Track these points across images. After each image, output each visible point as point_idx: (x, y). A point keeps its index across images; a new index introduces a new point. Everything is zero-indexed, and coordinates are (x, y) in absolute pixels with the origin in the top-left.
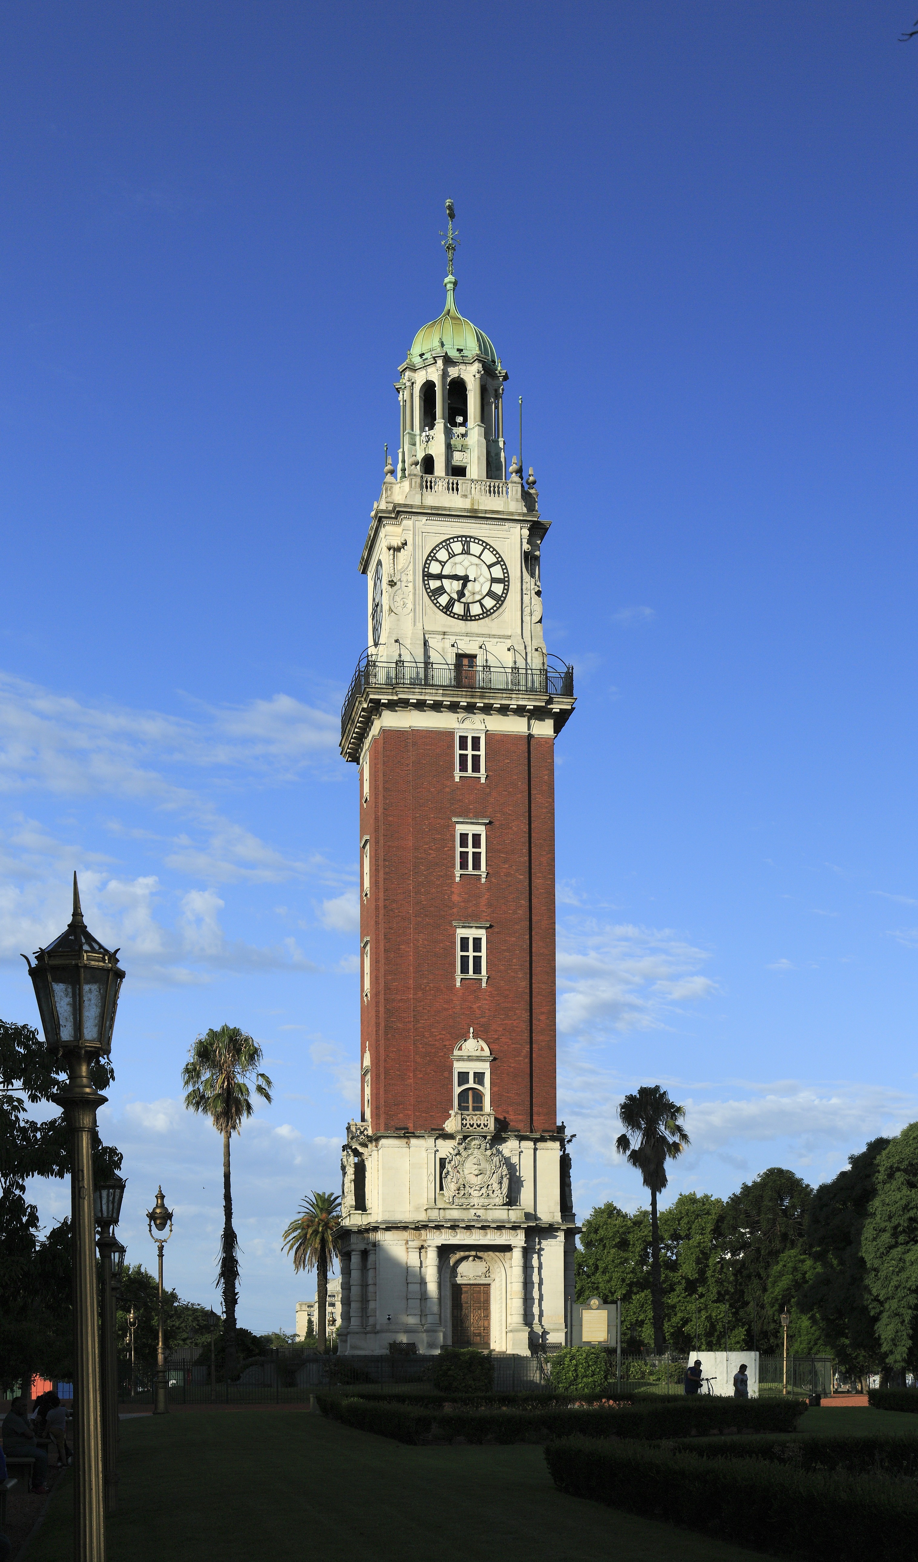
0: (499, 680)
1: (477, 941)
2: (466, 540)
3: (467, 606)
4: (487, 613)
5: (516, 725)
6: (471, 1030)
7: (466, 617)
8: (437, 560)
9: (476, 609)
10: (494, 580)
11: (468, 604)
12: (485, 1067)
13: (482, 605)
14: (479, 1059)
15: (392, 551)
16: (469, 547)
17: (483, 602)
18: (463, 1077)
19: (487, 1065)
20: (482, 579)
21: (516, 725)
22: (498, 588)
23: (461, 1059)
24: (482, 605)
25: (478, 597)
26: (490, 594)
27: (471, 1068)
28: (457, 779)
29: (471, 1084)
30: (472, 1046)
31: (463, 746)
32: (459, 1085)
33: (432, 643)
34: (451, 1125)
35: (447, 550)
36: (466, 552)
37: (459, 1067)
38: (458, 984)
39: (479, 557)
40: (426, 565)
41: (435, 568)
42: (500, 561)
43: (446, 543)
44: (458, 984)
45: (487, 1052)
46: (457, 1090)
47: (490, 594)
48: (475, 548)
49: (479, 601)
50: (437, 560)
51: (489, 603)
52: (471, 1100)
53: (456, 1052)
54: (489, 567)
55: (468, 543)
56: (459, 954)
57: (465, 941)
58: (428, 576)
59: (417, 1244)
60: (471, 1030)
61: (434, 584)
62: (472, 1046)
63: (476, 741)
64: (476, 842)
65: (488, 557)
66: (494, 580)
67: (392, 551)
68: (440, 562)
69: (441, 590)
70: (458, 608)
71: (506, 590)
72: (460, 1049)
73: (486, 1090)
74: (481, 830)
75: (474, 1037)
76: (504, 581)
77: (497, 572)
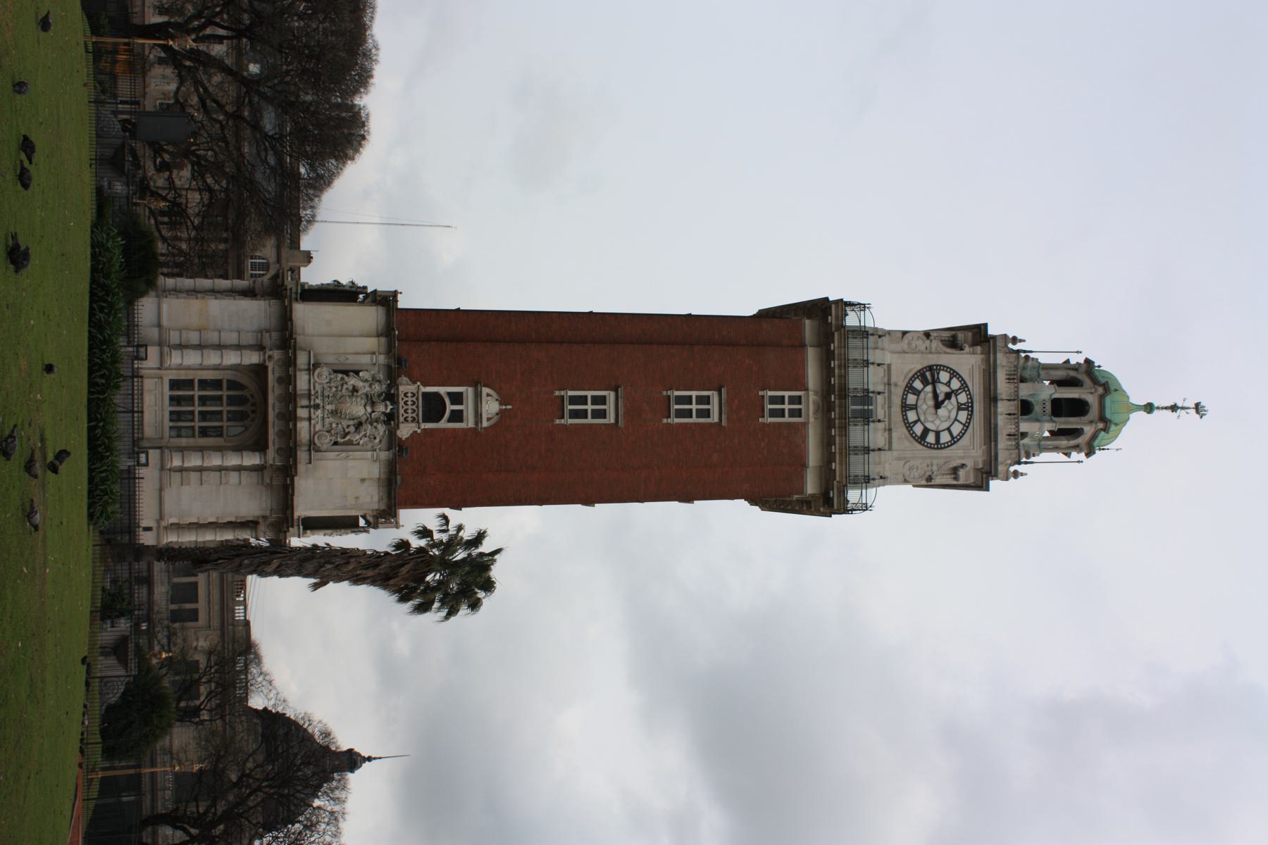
0: (856, 435)
1: (602, 414)
2: (969, 407)
3: (914, 407)
4: (909, 426)
5: (813, 457)
7: (905, 407)
9: (912, 416)
10: (938, 434)
12: (469, 422)
13: (916, 422)
14: (478, 416)
17: (919, 424)
18: (457, 398)
19: (471, 424)
20: (937, 422)
21: (813, 457)
22: (931, 438)
23: (478, 396)
24: (916, 422)
25: (922, 418)
26: (926, 431)
27: (468, 408)
28: (761, 393)
29: (450, 407)
30: (491, 407)
31: (793, 400)
32: (449, 394)
33: (881, 369)
34: (406, 387)
36: (959, 409)
37: (468, 392)
38: (557, 393)
39: (956, 420)
40: (946, 368)
41: (944, 376)
42: (954, 440)
43: (964, 386)
44: (557, 393)
45: (485, 424)
46: (443, 390)
47: (926, 431)
48: (963, 416)
49: (919, 420)
51: (918, 429)
52: (433, 408)
53: (485, 390)
54: (948, 429)
55: (966, 409)
56: (589, 394)
57: (603, 400)
59: (267, 341)
62: (491, 407)
63: (797, 413)
64: (702, 414)
65: (956, 429)
66: (938, 434)
71: (930, 446)
72: (488, 395)
73: (443, 424)
74: (715, 418)
75: (501, 413)
76: (938, 445)
77: (945, 438)
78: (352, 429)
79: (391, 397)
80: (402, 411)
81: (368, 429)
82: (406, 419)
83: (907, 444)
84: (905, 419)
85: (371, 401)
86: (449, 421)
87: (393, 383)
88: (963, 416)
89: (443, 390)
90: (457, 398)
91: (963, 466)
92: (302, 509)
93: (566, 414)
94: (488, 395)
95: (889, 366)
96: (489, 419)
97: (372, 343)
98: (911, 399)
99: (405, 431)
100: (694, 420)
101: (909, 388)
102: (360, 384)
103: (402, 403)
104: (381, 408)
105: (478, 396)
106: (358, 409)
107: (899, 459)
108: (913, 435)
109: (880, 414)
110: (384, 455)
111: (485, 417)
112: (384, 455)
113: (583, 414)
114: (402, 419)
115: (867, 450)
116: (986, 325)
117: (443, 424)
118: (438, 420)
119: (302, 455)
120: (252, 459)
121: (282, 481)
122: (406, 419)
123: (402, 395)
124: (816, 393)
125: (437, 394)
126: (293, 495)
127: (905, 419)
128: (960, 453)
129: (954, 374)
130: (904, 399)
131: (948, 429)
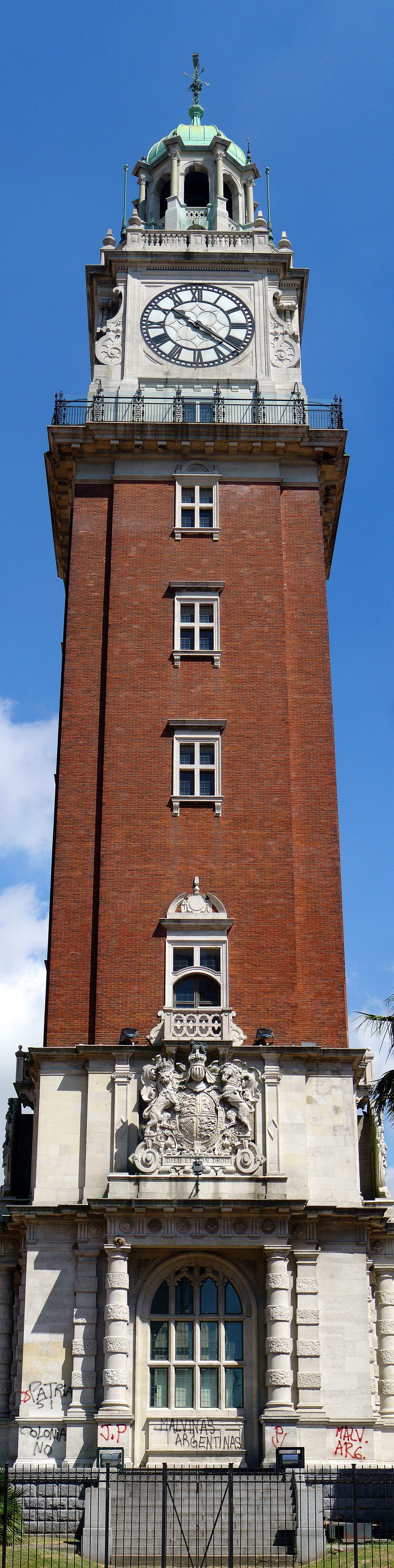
6: (197, 881)
7: (198, 363)
8: (159, 308)
10: (234, 326)
11: (199, 350)
15: (105, 312)
16: (200, 295)
22: (240, 334)
29: (197, 967)
32: (176, 969)
35: (173, 299)
39: (214, 304)
42: (241, 306)
46: (171, 978)
50: (159, 308)
54: (227, 313)
58: (145, 324)
60: (197, 881)
61: (154, 333)
65: (227, 304)
66: (234, 326)
67: (105, 312)
68: (164, 311)
69: (164, 338)
70: (186, 356)
72: (179, 910)
76: (250, 325)
77: (239, 317)
78: (232, 1114)
79: (181, 1053)
80: (205, 1037)
81: (232, 1089)
82: (216, 1031)
83: (247, 362)
84: (212, 364)
85: (189, 1085)
86: (218, 969)
87: (160, 1047)
88: (209, 296)
89: (171, 978)
90: (183, 957)
91: (275, 299)
92: (353, 1199)
93: (207, 798)
94: (179, 910)
95: (141, 381)
96: (215, 910)
97: (97, 1081)
98: (186, 356)
99: (236, 1036)
100: (215, 625)
101: (173, 357)
102: (162, 1100)
103: (190, 1037)
104: (199, 1068)
105: (181, 926)
106: (204, 1102)
107: (268, 373)
108: (235, 354)
109: (208, 393)
110: (271, 1069)
111: (212, 916)
112: (271, 1069)
113: (207, 776)
114: (217, 1038)
115: (257, 401)
116: (88, 268)
117: (222, 978)
118: (217, 986)
119: (275, 1192)
120: (280, 1271)
121: (317, 1228)
122: (216, 1031)
123: (180, 1037)
124: (178, 468)
125: (177, 986)
126: (334, 1209)
127: (212, 364)
128: (259, 299)
129: (153, 305)
130: (186, 364)
131: (227, 313)
